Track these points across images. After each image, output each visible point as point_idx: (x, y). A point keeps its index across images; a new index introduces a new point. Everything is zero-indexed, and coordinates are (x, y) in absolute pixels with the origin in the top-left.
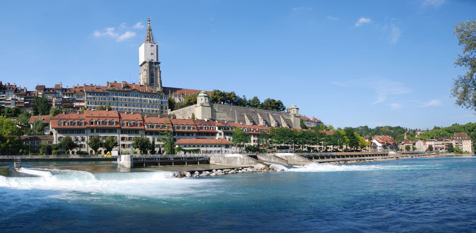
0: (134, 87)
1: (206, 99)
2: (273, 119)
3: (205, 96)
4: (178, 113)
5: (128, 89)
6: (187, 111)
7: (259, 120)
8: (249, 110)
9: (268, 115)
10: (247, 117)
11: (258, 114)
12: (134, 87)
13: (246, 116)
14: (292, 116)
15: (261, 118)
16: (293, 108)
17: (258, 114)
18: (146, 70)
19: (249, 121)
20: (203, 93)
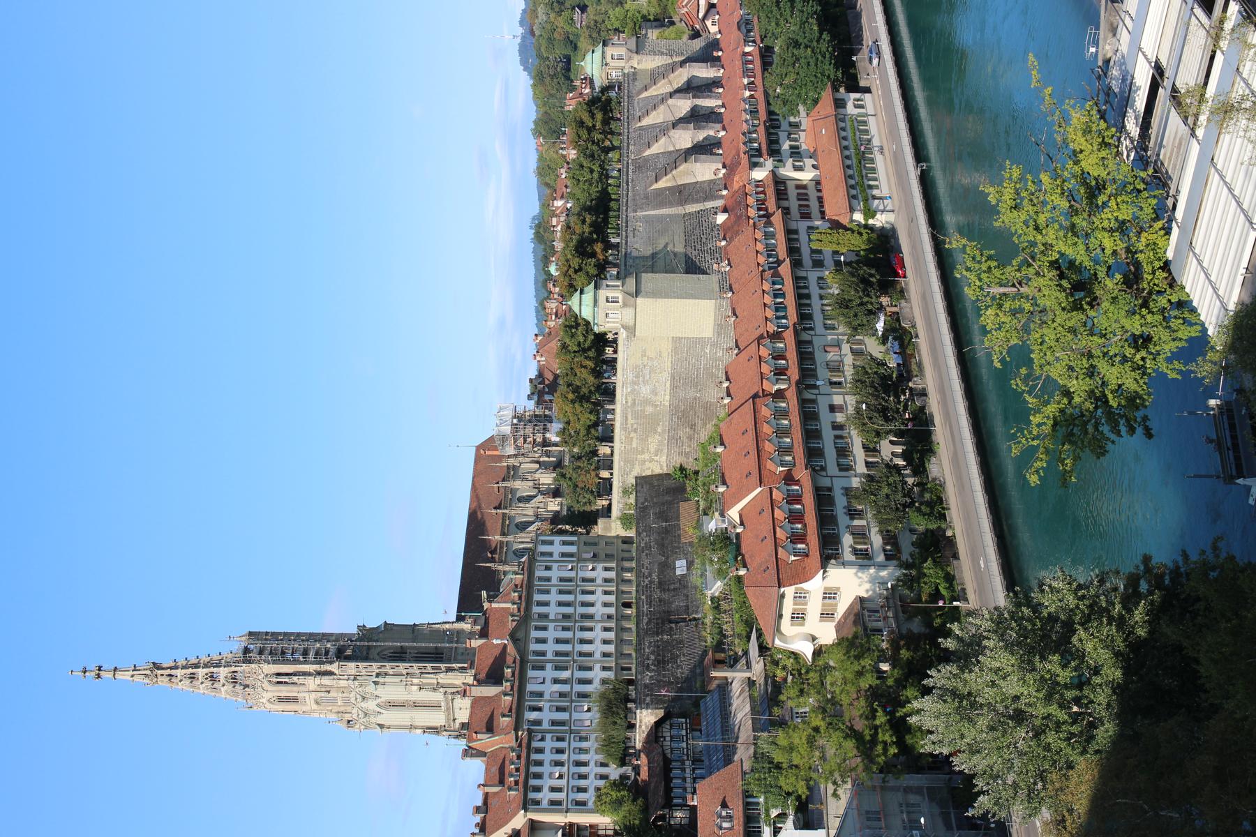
0: (499, 642)
1: (607, 286)
2: (662, 108)
3: (596, 287)
4: (629, 462)
5: (509, 660)
6: (634, 403)
7: (672, 149)
8: (633, 180)
9: (641, 128)
10: (664, 179)
11: (646, 154)
12: (499, 642)
13: (662, 184)
14: (636, 66)
15: (663, 140)
16: (603, 57)
17: (648, 153)
18: (378, 675)
19: (683, 167)
20: (583, 296)
